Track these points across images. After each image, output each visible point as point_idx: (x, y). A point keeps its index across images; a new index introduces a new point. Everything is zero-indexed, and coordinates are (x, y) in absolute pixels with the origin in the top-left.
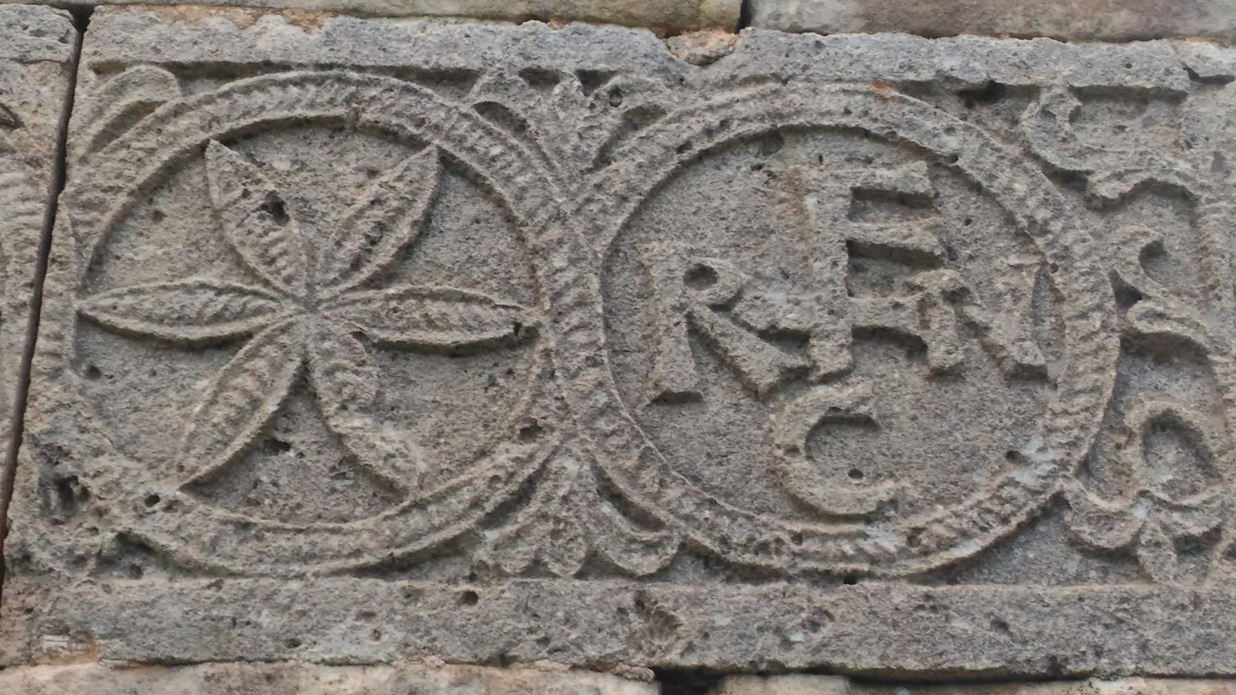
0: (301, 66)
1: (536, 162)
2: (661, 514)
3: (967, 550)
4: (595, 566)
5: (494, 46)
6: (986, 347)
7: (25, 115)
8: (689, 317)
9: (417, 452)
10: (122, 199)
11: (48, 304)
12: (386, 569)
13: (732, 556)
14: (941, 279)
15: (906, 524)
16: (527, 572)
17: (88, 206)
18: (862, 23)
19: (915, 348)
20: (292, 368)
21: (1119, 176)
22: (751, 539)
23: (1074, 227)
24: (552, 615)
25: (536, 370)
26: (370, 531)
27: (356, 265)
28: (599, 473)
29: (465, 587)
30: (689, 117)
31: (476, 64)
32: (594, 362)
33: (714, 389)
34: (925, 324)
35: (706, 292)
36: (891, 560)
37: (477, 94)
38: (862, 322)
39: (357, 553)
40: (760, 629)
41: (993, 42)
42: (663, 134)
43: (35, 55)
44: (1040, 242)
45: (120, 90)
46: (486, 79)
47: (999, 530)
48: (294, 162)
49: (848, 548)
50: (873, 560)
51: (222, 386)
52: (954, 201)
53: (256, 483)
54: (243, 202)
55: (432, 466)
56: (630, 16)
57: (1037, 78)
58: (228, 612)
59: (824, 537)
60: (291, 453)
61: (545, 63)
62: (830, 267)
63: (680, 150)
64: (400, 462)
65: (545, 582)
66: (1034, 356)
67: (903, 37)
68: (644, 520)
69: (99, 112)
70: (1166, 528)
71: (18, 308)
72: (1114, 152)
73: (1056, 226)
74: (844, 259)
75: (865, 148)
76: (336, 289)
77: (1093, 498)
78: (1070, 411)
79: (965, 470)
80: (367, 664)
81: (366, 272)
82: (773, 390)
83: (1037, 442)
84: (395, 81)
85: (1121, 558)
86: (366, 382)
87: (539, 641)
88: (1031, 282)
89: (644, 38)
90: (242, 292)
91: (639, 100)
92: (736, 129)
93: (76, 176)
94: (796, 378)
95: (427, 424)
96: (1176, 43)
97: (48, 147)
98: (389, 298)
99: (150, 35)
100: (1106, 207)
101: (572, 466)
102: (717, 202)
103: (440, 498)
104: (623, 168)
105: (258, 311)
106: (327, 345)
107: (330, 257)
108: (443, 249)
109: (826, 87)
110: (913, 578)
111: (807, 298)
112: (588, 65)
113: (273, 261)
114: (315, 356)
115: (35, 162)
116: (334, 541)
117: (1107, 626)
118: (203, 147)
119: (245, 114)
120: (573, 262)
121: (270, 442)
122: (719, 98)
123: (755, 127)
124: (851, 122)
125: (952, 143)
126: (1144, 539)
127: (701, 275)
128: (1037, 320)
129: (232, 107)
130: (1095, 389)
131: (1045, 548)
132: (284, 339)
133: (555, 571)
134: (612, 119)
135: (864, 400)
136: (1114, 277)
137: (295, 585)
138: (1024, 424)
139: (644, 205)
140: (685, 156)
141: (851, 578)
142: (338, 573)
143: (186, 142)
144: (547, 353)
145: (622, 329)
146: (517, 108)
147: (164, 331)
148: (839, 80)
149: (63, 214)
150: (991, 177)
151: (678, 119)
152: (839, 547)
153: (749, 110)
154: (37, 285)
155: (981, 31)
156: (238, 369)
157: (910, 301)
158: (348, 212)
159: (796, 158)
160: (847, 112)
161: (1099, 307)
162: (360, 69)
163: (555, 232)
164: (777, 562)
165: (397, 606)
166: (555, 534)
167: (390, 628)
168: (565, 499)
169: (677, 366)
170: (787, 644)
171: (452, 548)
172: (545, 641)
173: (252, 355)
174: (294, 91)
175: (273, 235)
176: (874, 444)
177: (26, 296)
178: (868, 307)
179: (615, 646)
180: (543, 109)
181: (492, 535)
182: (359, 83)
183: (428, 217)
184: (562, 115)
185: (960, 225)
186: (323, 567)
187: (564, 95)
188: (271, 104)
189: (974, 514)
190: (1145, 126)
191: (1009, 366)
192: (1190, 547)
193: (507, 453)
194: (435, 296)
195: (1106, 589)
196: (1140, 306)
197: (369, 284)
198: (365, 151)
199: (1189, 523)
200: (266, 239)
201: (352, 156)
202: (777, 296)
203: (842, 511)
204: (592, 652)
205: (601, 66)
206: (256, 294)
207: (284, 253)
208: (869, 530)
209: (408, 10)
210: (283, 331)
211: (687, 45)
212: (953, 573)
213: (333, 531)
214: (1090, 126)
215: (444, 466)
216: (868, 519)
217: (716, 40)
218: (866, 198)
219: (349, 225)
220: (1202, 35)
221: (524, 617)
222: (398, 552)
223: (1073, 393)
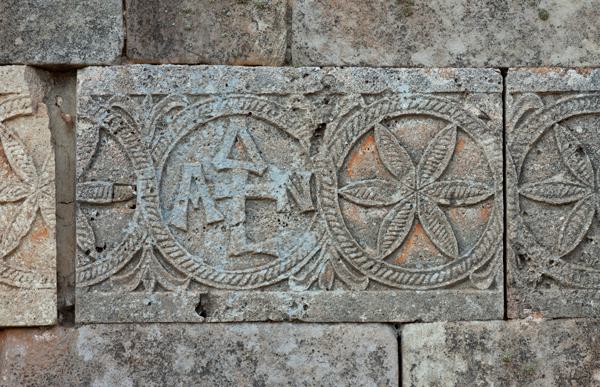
7: (491, 115)
10: (528, 148)
11: (509, 191)
17: (517, 151)
43: (491, 90)
45: (522, 103)
69: (516, 112)
71: (499, 192)
90: (573, 185)
93: (510, 139)
97: (500, 127)
99: (528, 81)
105: (580, 192)
115: (496, 135)
118: (553, 126)
143: (548, 124)
147: (549, 200)
149: (508, 155)
154: (504, 183)
173: (578, 209)
175: (581, 162)
177: (501, 188)
200: (579, 164)
206: (578, 186)
207: (585, 169)
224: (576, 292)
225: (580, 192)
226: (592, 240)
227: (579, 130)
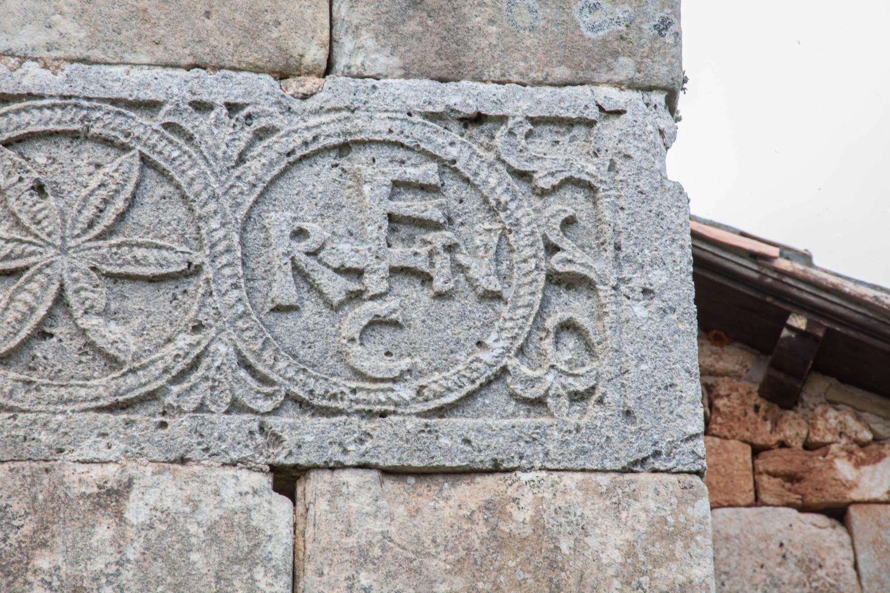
0: (51, 96)
1: (200, 161)
2: (275, 377)
3: (451, 398)
4: (236, 407)
5: (173, 85)
6: (467, 279)
8: (293, 259)
9: (131, 340)
12: (111, 409)
13: (315, 402)
14: (439, 239)
15: (416, 384)
16: (196, 410)
18: (402, 72)
19: (426, 279)
20: (54, 288)
21: (552, 174)
22: (327, 392)
23: (522, 206)
24: (211, 434)
25: (201, 291)
26: (104, 385)
27: (91, 225)
28: (239, 353)
29: (159, 419)
30: (294, 131)
31: (161, 97)
32: (235, 286)
33: (307, 303)
34: (432, 265)
35: (303, 244)
36: (407, 404)
37: (162, 116)
38: (395, 264)
39: (97, 399)
40: (331, 443)
41: (481, 86)
42: (278, 144)
44: (502, 215)
46: (167, 107)
47: (469, 387)
48: (49, 158)
49: (382, 397)
50: (397, 404)
51: (12, 299)
52: (453, 186)
53: (34, 357)
54: (20, 185)
55: (139, 348)
56: (258, 67)
57: (506, 111)
58: (21, 433)
59: (369, 391)
60: (54, 339)
61: (205, 98)
62: (377, 229)
63: (289, 155)
64: (121, 346)
65: (207, 416)
66: (495, 285)
67: (427, 82)
68: (264, 380)
70: (564, 387)
72: (551, 157)
73: (512, 206)
74: (386, 224)
75: (401, 154)
76: (79, 240)
77: (525, 369)
78: (512, 318)
79: (452, 352)
80: (102, 462)
81: (97, 230)
82: (342, 304)
83: (494, 336)
84: (111, 107)
85: (538, 403)
86: (99, 297)
87: (203, 450)
88: (496, 240)
89: (266, 81)
90: (21, 242)
91: (263, 122)
92: (323, 142)
94: (355, 297)
95: (136, 323)
96: (593, 88)
98: (111, 246)
100: (543, 193)
101: (223, 349)
102: (310, 188)
103: (143, 367)
104: (254, 166)
105: (32, 254)
106: (75, 275)
107: (75, 220)
108: (143, 215)
109: (378, 115)
110: (418, 415)
111: (363, 248)
112: (231, 99)
113: (39, 222)
114: (68, 282)
116: (83, 392)
117: (527, 442)
119: (18, 127)
120: (223, 225)
121: (41, 334)
122: (313, 121)
123: (334, 141)
124: (393, 138)
125: (453, 152)
126: (551, 393)
127: (300, 234)
128: (498, 262)
129: (9, 123)
130: (530, 305)
131: (496, 398)
132: (48, 271)
133: (213, 410)
134: (246, 135)
135: (395, 311)
136: (545, 237)
137: (60, 417)
138: (489, 325)
139: (266, 189)
140: (291, 159)
141: (383, 415)
142: (85, 410)
144: (207, 281)
145: (253, 265)
146: (188, 127)
148: (386, 111)
150: (476, 174)
151: (288, 135)
152: (378, 397)
153: (331, 129)
155: (474, 79)
156: (20, 289)
157: (424, 251)
158: (84, 192)
159: (359, 160)
160: (390, 131)
161: (535, 256)
162: (89, 99)
163: (212, 206)
164: (341, 405)
165: (121, 430)
166: (213, 388)
167: (117, 442)
168: (219, 368)
169: (284, 289)
170: (345, 451)
171: (152, 396)
172: (207, 450)
173: (28, 281)
174: (48, 113)
175: (39, 206)
176: (400, 336)
178: (399, 254)
179: (247, 453)
180: (203, 128)
181: (175, 389)
182: (88, 108)
183: (134, 195)
184: (216, 131)
185: (456, 204)
186: (76, 407)
187: (217, 119)
188: (33, 120)
189: (455, 378)
190: (571, 141)
191: (480, 291)
192: (577, 397)
193: (184, 340)
194: (139, 245)
195: (526, 421)
196: (559, 255)
197: (98, 237)
198: (91, 152)
199: (577, 384)
200: (35, 209)
201: (85, 155)
202: (345, 247)
203: (379, 376)
204: (234, 456)
205: (240, 100)
206: (30, 243)
207: (47, 217)
208: (396, 387)
209: (117, 60)
210: (48, 266)
211: (293, 85)
212: (441, 412)
213: (81, 386)
214: (538, 140)
215: (147, 348)
216: (394, 380)
217: (311, 83)
218: (399, 186)
219: (85, 200)
220: (609, 82)
221: (195, 436)
222: (121, 399)
223: (515, 308)
224: (14, 417)
225: (32, 254)
226: (51, 335)
227: (41, 159)
